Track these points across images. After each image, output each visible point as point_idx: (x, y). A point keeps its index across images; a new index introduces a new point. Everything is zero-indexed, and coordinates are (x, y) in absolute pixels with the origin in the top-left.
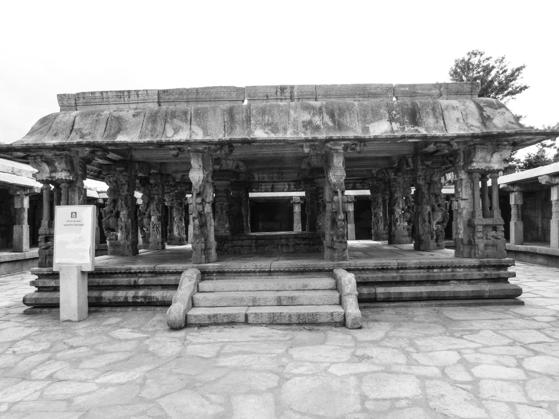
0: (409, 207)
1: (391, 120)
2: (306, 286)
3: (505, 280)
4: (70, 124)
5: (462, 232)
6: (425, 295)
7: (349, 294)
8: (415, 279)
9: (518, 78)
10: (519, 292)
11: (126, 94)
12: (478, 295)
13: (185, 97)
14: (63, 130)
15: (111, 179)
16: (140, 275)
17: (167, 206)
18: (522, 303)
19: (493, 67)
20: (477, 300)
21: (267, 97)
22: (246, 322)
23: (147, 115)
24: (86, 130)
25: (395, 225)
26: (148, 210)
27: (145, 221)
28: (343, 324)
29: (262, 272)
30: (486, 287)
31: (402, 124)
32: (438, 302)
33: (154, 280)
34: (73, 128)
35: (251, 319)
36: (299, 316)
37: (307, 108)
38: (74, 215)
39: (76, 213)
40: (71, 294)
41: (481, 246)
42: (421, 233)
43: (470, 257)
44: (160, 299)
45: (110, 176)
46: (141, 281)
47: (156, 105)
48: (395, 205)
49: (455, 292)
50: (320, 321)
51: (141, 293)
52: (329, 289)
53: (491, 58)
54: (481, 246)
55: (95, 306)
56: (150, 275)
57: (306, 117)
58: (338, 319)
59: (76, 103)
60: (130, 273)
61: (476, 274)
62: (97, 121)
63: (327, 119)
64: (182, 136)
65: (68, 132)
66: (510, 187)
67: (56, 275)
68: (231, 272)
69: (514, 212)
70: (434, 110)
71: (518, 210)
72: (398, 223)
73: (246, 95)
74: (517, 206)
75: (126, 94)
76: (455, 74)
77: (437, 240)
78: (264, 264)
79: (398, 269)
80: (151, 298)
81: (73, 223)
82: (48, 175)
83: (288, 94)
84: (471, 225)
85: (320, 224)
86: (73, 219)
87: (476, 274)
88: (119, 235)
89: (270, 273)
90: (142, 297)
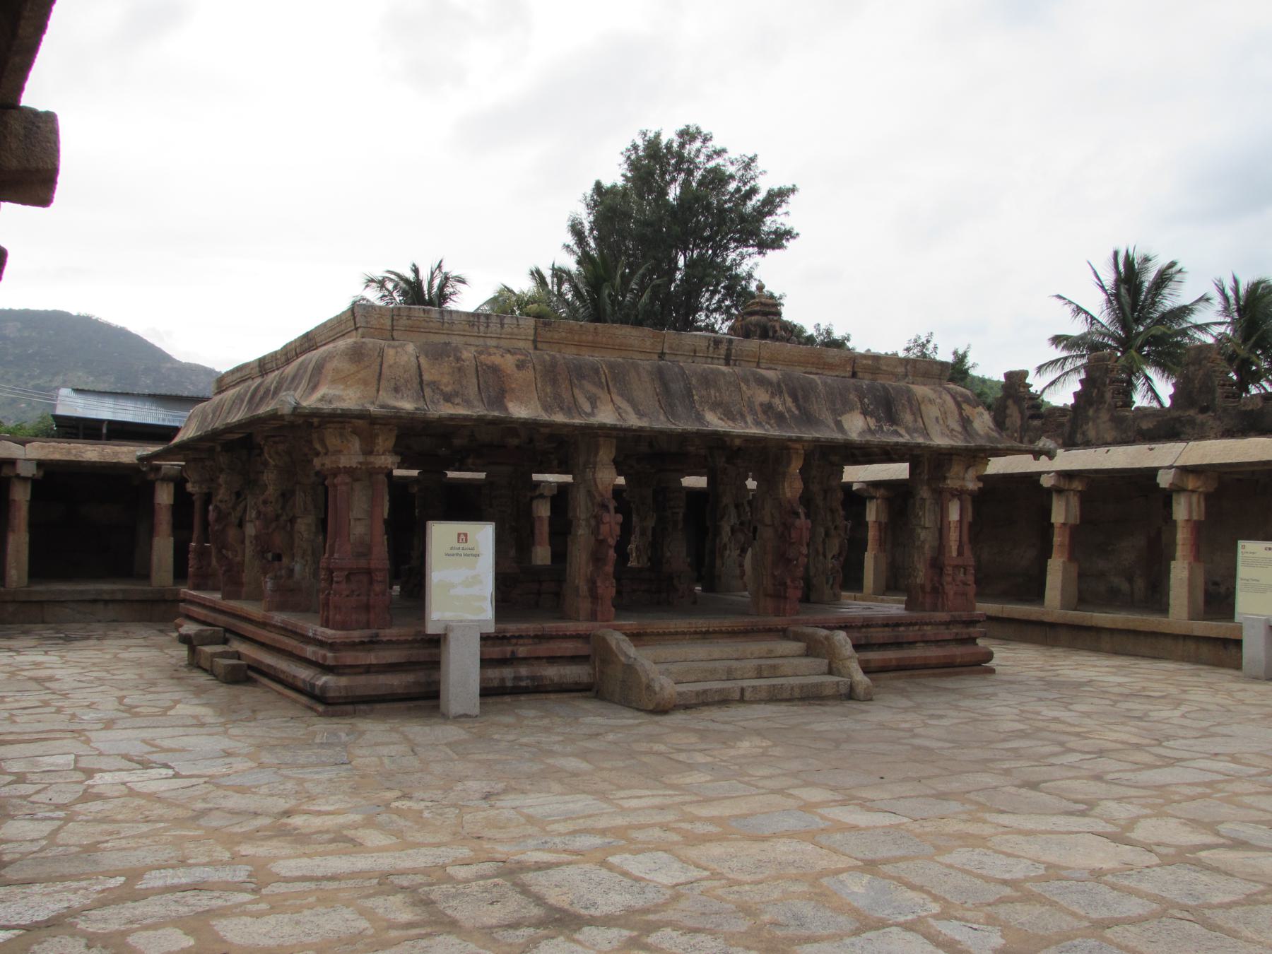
0: (742, 524)
1: (865, 413)
2: (771, 651)
3: (971, 640)
4: (414, 370)
5: (921, 574)
6: (894, 663)
7: (850, 658)
8: (881, 641)
9: (779, 211)
10: (989, 656)
11: (482, 319)
12: (657, 718)
13: (576, 338)
14: (407, 381)
15: (281, 447)
16: (514, 641)
17: (191, 495)
18: (992, 671)
19: (732, 177)
20: (949, 667)
21: (695, 352)
22: (742, 700)
23: (538, 367)
24: (446, 386)
25: (722, 557)
26: (240, 508)
27: (232, 533)
28: (850, 695)
29: (705, 635)
30: (958, 651)
31: (878, 420)
32: (908, 673)
33: (544, 649)
34: (421, 382)
35: (748, 695)
36: (802, 687)
37: (762, 382)
38: (463, 537)
39: (466, 535)
40: (462, 671)
41: (951, 593)
42: (812, 574)
43: (934, 608)
44: (556, 679)
45: (277, 439)
46: (522, 651)
47: (529, 345)
48: (722, 518)
49: (926, 658)
50: (825, 693)
51: (524, 671)
52: (799, 656)
53: (724, 151)
54: (951, 593)
55: (487, 692)
56: (531, 641)
57: (762, 396)
58: (844, 690)
59: (392, 326)
60: (504, 638)
61: (946, 633)
62: (459, 369)
63: (789, 401)
64: (606, 416)
65: (415, 385)
66: (871, 490)
67: (437, 642)
68: (652, 634)
69: (872, 534)
70: (909, 400)
71: (880, 530)
72: (728, 552)
73: (666, 345)
74: (880, 524)
75: (482, 319)
76: (634, 165)
77: (832, 587)
78: (701, 623)
79: (863, 626)
80: (542, 678)
81: (461, 552)
82: (361, 459)
83: (723, 351)
84: (937, 565)
85: (669, 554)
86: (462, 545)
87: (946, 633)
88: (297, 568)
89: (705, 635)
90: (528, 678)
